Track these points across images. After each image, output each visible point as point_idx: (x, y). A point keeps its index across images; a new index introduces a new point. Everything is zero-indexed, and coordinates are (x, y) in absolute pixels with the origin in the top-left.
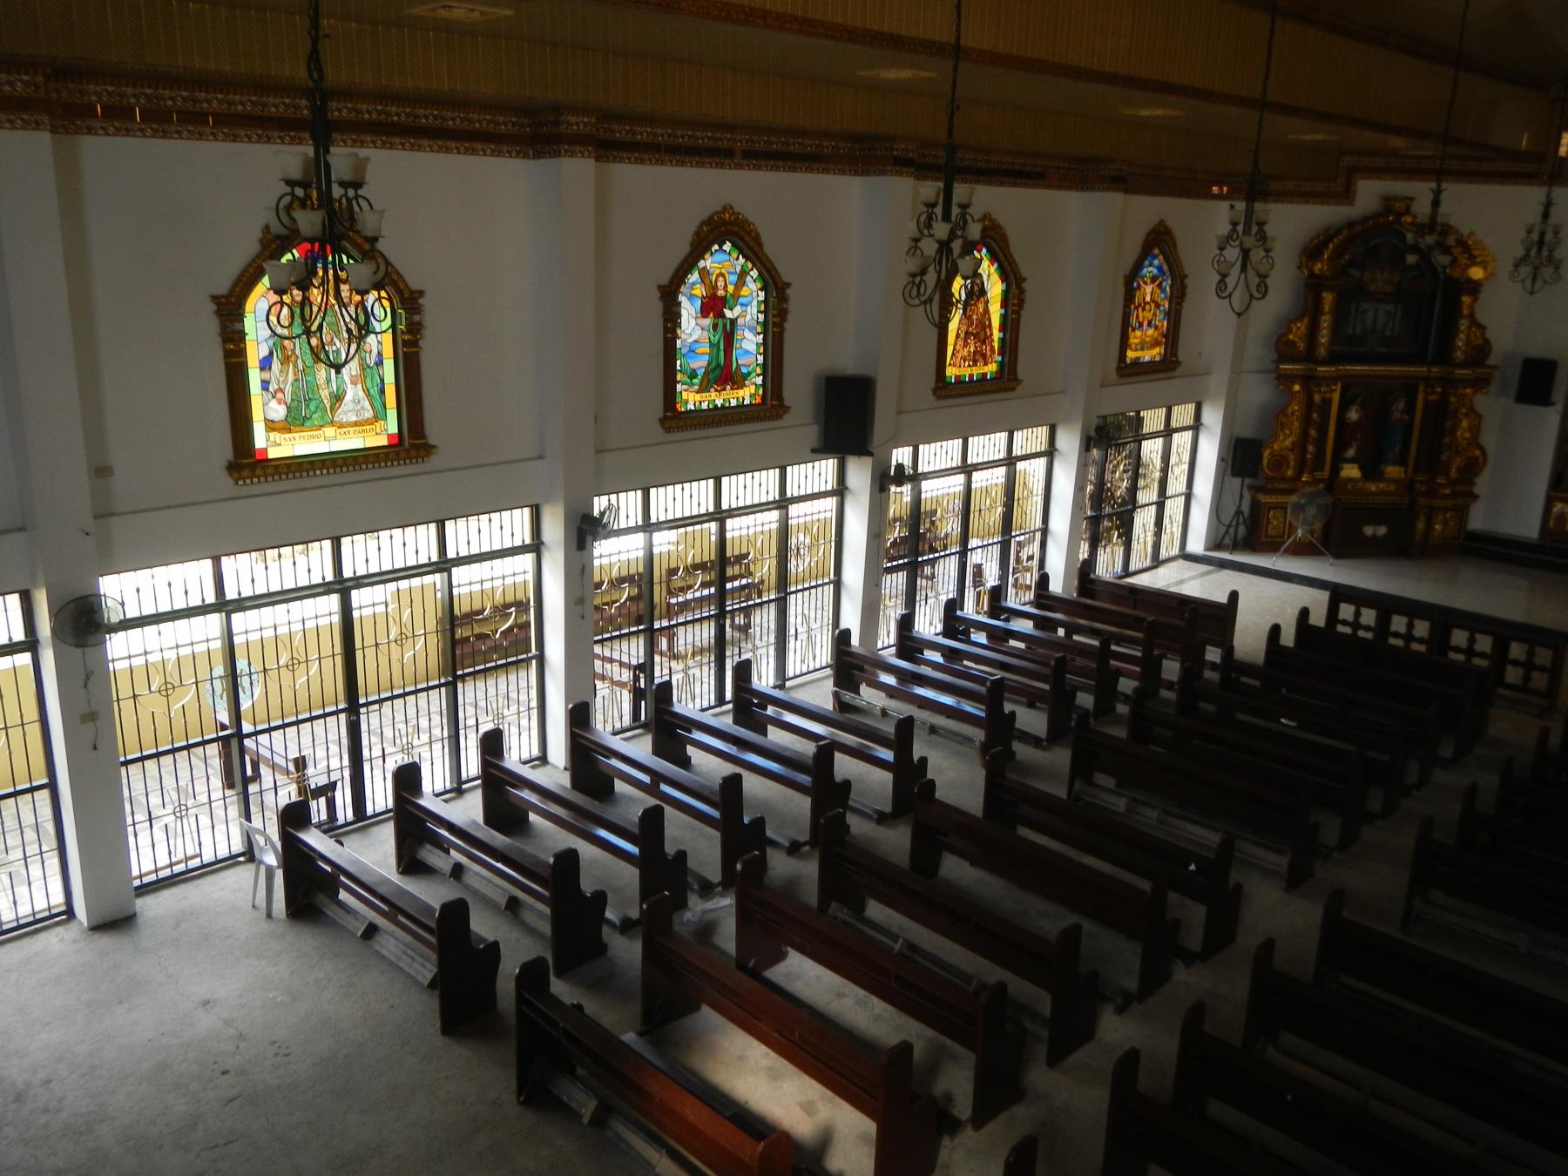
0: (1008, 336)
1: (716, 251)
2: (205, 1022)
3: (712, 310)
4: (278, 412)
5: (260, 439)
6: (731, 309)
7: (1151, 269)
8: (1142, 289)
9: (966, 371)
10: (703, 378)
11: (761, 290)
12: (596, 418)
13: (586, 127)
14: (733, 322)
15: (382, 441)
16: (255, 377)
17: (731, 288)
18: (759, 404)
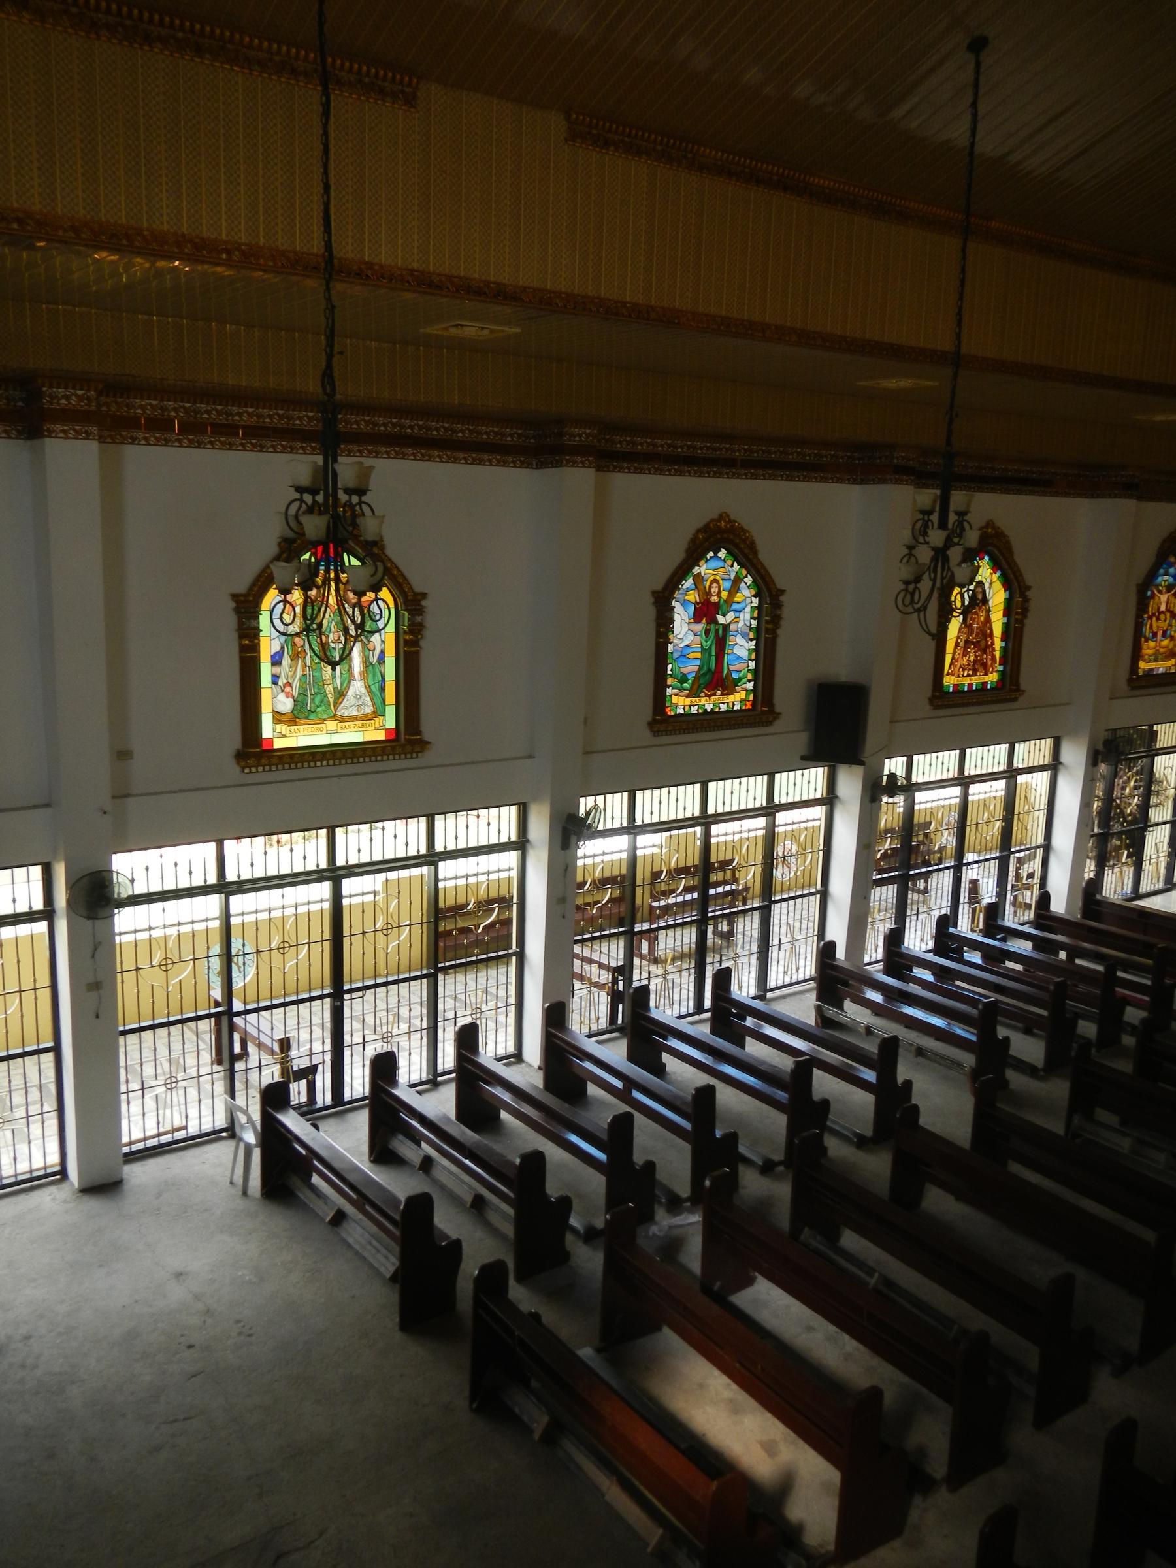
0: (1010, 646)
1: (711, 557)
2: (177, 1294)
3: (705, 616)
4: (285, 704)
5: (268, 728)
6: (724, 615)
7: (1166, 577)
8: (1157, 598)
10: (693, 682)
11: (755, 596)
12: (586, 720)
13: (472, 434)
15: (380, 736)
16: (266, 672)
17: (724, 594)
18: (749, 710)
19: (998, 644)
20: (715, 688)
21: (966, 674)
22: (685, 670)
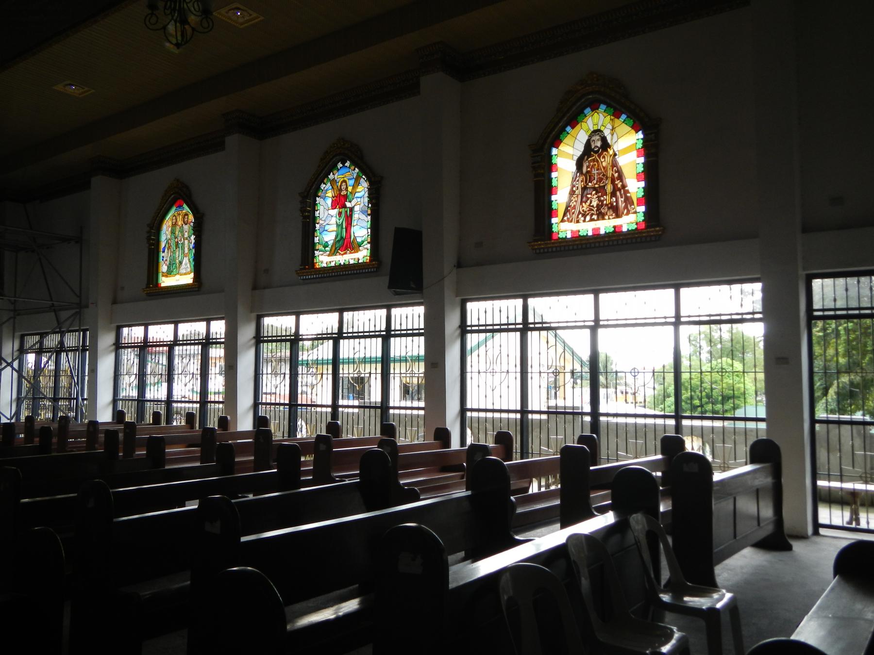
1: (341, 168)
6: (350, 202)
9: (586, 228)
10: (332, 246)
14: (352, 209)
17: (350, 189)
19: (635, 187)
20: (346, 249)
21: (588, 218)
22: (326, 239)
